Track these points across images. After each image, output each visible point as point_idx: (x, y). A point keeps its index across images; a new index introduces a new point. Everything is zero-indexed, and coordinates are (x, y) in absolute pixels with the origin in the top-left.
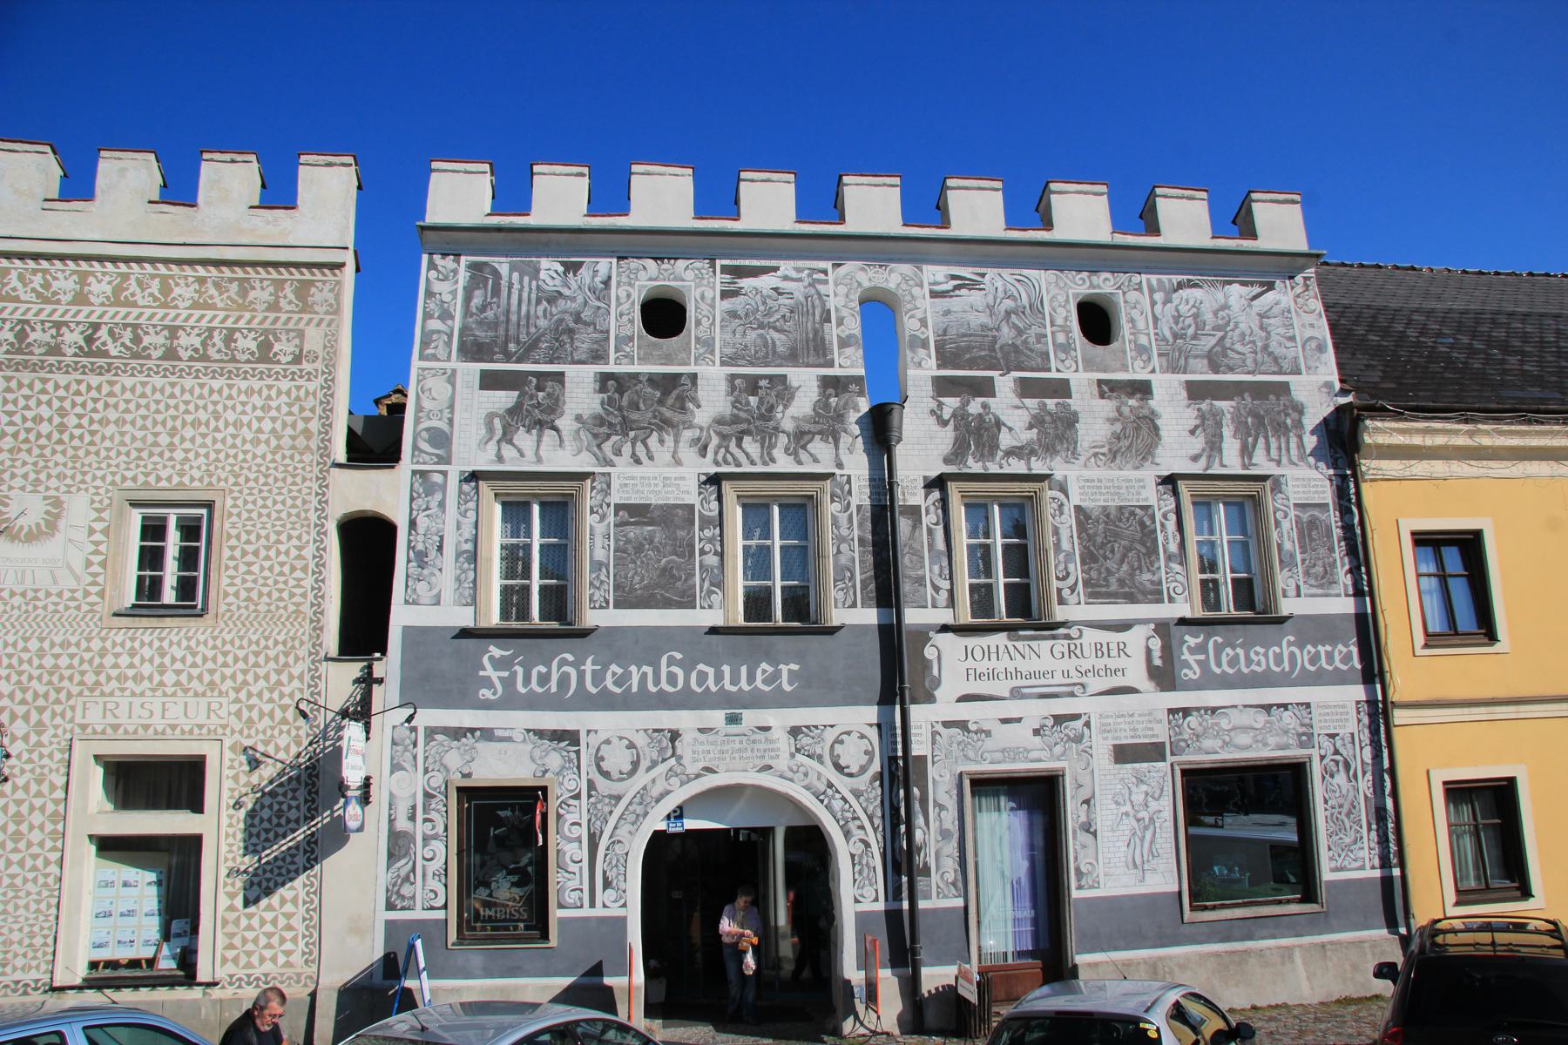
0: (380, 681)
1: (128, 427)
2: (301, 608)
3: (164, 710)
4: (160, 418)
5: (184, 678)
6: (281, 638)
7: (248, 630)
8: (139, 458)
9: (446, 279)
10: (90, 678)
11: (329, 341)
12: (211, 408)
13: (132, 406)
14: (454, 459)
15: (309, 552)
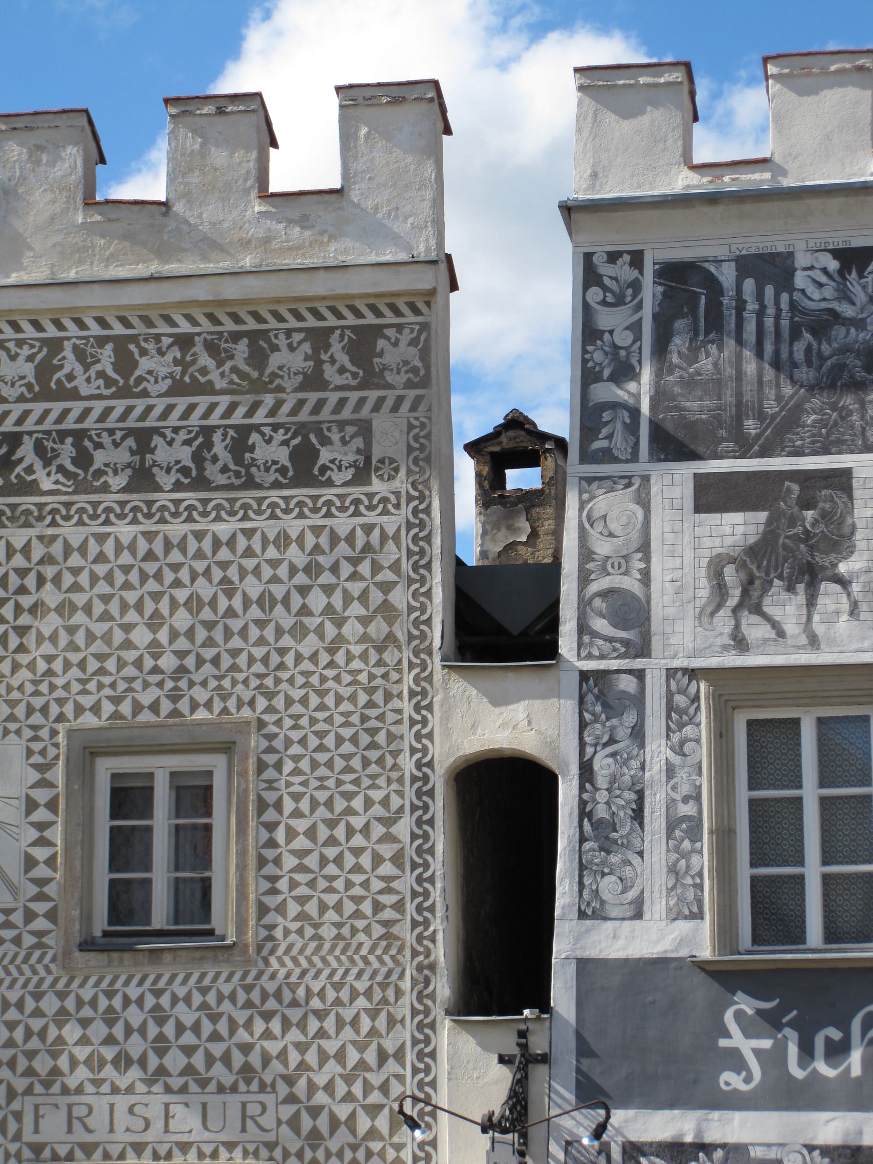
0: (544, 1059)
1: (79, 618)
2: (395, 930)
3: (167, 1117)
4: (131, 597)
5: (198, 1061)
6: (361, 986)
7: (304, 973)
8: (102, 671)
9: (620, 301)
10: (42, 1064)
11: (416, 438)
12: (217, 574)
13: (84, 579)
14: (656, 644)
15: (404, 828)
